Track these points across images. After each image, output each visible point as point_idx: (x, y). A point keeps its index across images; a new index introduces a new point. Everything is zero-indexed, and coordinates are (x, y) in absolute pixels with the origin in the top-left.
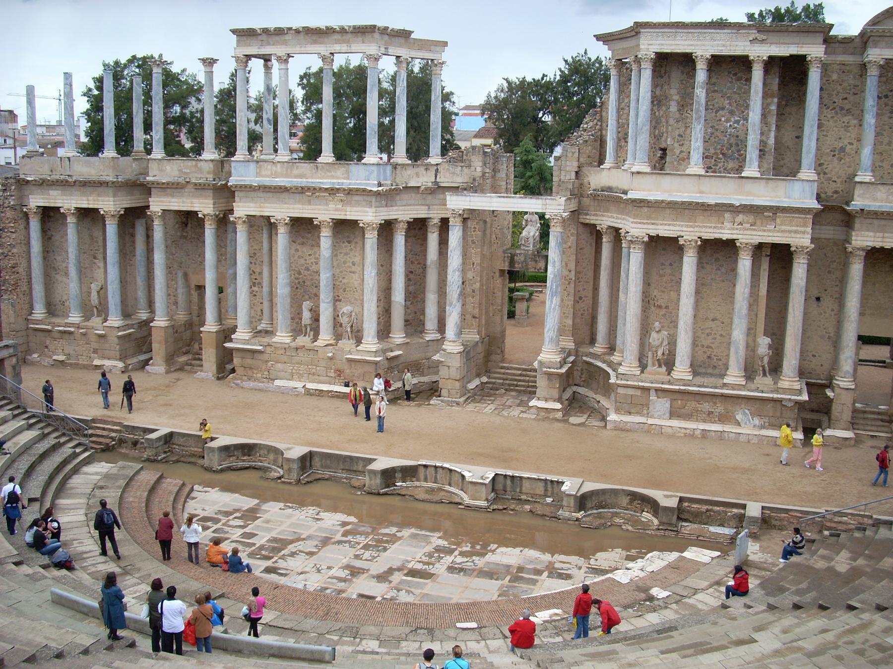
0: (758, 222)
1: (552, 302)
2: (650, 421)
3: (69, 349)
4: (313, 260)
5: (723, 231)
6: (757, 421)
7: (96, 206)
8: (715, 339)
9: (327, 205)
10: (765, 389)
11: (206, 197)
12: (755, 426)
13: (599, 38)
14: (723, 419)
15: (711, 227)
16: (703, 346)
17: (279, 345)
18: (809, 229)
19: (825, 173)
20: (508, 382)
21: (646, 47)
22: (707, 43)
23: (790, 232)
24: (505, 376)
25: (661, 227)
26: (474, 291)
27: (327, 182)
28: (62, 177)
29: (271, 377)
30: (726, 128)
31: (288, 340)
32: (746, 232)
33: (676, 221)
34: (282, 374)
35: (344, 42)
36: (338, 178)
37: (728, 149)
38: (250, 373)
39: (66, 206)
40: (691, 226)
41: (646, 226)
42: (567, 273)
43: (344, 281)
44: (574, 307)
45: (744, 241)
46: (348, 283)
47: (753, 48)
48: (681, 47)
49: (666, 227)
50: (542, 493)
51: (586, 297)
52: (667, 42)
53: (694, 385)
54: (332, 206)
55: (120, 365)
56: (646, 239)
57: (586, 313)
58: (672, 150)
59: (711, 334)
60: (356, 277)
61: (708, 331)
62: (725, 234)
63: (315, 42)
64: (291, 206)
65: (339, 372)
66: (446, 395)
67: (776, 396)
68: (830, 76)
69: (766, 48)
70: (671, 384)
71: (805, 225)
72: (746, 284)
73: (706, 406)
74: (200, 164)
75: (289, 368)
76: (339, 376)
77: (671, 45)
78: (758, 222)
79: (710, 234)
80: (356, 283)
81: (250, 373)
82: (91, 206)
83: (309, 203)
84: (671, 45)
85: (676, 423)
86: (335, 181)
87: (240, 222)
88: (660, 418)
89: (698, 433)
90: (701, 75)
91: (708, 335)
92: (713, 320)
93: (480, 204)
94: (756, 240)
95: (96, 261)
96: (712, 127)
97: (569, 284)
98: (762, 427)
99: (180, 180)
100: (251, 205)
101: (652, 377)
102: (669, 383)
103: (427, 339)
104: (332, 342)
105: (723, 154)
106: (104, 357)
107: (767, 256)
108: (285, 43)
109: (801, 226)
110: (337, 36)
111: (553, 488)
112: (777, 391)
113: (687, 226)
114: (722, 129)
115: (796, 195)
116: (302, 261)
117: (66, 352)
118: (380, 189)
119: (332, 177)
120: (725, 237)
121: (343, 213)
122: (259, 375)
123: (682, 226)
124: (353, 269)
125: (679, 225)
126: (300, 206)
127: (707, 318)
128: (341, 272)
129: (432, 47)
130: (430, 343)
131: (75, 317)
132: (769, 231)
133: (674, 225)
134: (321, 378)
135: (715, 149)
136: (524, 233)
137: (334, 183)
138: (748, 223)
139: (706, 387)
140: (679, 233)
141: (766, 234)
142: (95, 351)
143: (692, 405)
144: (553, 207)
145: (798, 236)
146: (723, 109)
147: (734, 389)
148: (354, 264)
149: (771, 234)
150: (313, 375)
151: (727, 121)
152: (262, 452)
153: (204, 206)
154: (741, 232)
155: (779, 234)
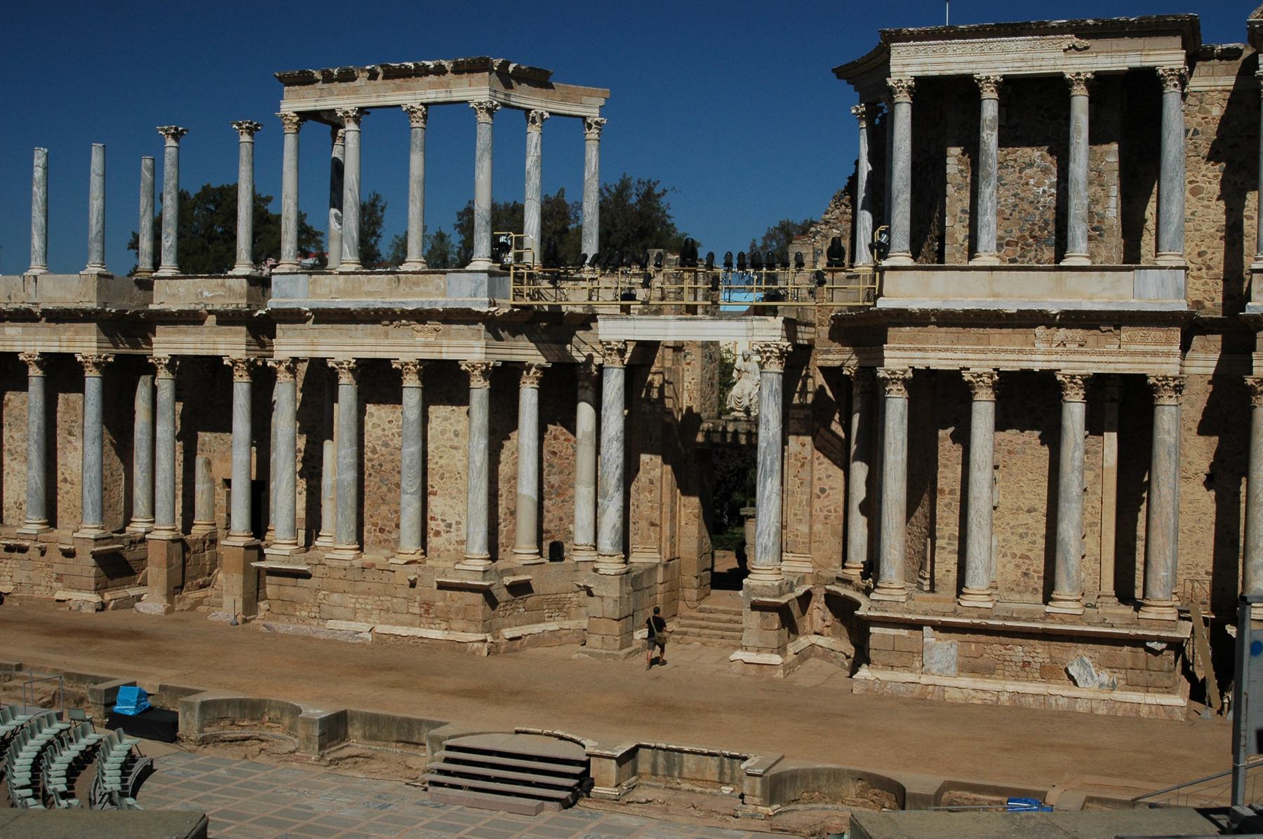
0: (1091, 341)
1: (764, 486)
2: (925, 680)
3: (21, 576)
4: (395, 430)
5: (1033, 357)
6: (1105, 677)
7: (71, 350)
8: (1034, 543)
9: (412, 337)
10: (1117, 621)
11: (236, 334)
12: (1101, 685)
13: (840, 72)
14: (1048, 673)
15: (1013, 352)
16: (1014, 556)
17: (335, 564)
19: (1209, 268)
20: (707, 631)
21: (900, 69)
22: (998, 57)
23: (1144, 354)
24: (703, 623)
25: (932, 355)
26: (651, 482)
27: (412, 303)
28: (24, 306)
29: (323, 615)
30: (1037, 196)
31: (349, 555)
32: (1071, 357)
34: (338, 611)
35: (441, 85)
36: (429, 294)
37: (1042, 229)
38: (290, 610)
39: (29, 350)
40: (982, 352)
41: (908, 354)
43: (441, 462)
44: (810, 503)
45: (1069, 372)
46: (448, 465)
47: (1068, 62)
48: (954, 66)
50: (716, 778)
51: (831, 489)
52: (934, 60)
53: (997, 617)
54: (420, 339)
55: (95, 598)
56: (910, 375)
57: (833, 515)
58: (952, 236)
59: (1027, 534)
60: (459, 454)
61: (1021, 530)
62: (1038, 363)
63: (399, 88)
64: (359, 341)
65: (427, 606)
66: (598, 644)
67: (1133, 632)
68: (1209, 112)
69: (1090, 60)
70: (959, 616)
71: (1168, 342)
72: (1076, 444)
73: (1019, 650)
74: (229, 282)
75: (350, 600)
76: (427, 612)
77: (939, 64)
78: (1091, 341)
79: (1012, 364)
80: (459, 464)
81: (290, 610)
82: (64, 350)
83: (386, 335)
84: (939, 64)
85: (966, 682)
86: (424, 299)
87: (282, 368)
88: (941, 673)
89: (1004, 698)
90: (990, 110)
91: (1021, 536)
92: (1029, 511)
93: (650, 332)
94: (1092, 369)
95: (72, 439)
96: (1015, 195)
97: (802, 466)
98: (1113, 687)
99: (198, 307)
100: (300, 341)
102: (955, 613)
103: (576, 559)
104: (417, 557)
105: (1034, 237)
106: (71, 588)
107: (1113, 400)
108: (356, 91)
109: (1161, 344)
110: (432, 78)
111: (732, 769)
112: (1136, 623)
113: (974, 352)
114: (1031, 197)
115: (1151, 292)
116: (379, 432)
117: (16, 580)
118: (492, 309)
119: (422, 294)
120: (1037, 367)
121: (437, 349)
122: (304, 613)
123: (966, 351)
124: (456, 442)
126: (372, 341)
127: (1019, 508)
128: (437, 448)
129: (584, 99)
130: (581, 566)
131: (33, 525)
132: (1110, 353)
134: (399, 616)
135: (1021, 230)
136: (735, 391)
137: (423, 303)
138: (1073, 341)
139: (1016, 619)
140: (963, 364)
142: (59, 578)
143: (994, 648)
144: (764, 332)
145: (1159, 360)
146: (1031, 165)
147: (1063, 622)
148: (456, 435)
149: (1113, 359)
150: (387, 612)
151: (1038, 185)
152: (272, 714)
153: (231, 346)
154: (1064, 358)
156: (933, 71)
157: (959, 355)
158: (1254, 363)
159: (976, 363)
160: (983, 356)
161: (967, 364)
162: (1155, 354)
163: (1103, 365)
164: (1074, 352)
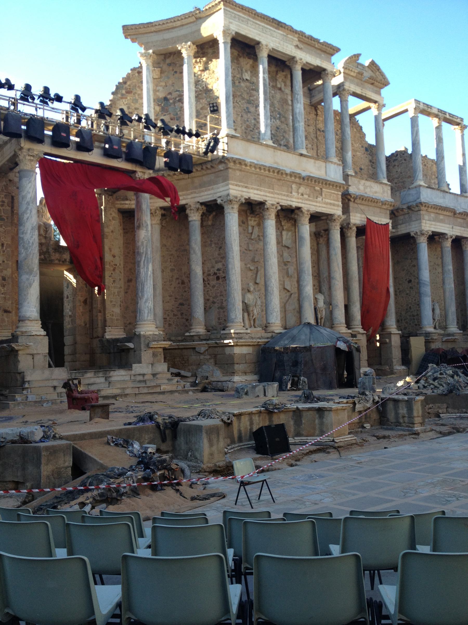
1: (148, 268)
15: (284, 195)
18: (340, 203)
23: (331, 204)
25: (251, 191)
33: (260, 187)
40: (272, 193)
41: (240, 189)
42: (112, 258)
49: (256, 192)
97: (114, 270)
101: (259, 335)
113: (269, 192)
120: (294, 205)
125: (264, 191)
132: (319, 202)
133: (261, 190)
138: (306, 194)
140: (265, 198)
141: (318, 204)
149: (321, 205)
154: (304, 202)
155: (324, 206)
156: (243, 32)
157: (262, 193)
158: (351, 217)
159: (270, 199)
160: (272, 195)
161: (267, 199)
162: (334, 205)
163: (317, 207)
164: (307, 200)
